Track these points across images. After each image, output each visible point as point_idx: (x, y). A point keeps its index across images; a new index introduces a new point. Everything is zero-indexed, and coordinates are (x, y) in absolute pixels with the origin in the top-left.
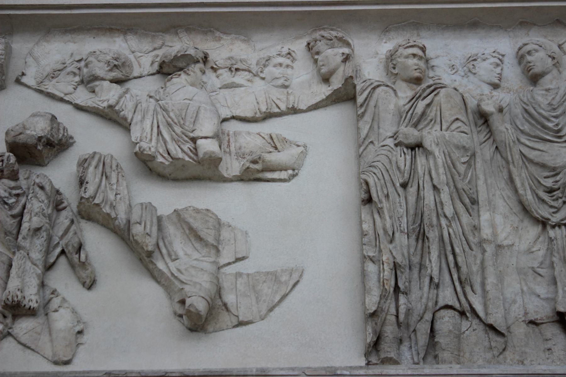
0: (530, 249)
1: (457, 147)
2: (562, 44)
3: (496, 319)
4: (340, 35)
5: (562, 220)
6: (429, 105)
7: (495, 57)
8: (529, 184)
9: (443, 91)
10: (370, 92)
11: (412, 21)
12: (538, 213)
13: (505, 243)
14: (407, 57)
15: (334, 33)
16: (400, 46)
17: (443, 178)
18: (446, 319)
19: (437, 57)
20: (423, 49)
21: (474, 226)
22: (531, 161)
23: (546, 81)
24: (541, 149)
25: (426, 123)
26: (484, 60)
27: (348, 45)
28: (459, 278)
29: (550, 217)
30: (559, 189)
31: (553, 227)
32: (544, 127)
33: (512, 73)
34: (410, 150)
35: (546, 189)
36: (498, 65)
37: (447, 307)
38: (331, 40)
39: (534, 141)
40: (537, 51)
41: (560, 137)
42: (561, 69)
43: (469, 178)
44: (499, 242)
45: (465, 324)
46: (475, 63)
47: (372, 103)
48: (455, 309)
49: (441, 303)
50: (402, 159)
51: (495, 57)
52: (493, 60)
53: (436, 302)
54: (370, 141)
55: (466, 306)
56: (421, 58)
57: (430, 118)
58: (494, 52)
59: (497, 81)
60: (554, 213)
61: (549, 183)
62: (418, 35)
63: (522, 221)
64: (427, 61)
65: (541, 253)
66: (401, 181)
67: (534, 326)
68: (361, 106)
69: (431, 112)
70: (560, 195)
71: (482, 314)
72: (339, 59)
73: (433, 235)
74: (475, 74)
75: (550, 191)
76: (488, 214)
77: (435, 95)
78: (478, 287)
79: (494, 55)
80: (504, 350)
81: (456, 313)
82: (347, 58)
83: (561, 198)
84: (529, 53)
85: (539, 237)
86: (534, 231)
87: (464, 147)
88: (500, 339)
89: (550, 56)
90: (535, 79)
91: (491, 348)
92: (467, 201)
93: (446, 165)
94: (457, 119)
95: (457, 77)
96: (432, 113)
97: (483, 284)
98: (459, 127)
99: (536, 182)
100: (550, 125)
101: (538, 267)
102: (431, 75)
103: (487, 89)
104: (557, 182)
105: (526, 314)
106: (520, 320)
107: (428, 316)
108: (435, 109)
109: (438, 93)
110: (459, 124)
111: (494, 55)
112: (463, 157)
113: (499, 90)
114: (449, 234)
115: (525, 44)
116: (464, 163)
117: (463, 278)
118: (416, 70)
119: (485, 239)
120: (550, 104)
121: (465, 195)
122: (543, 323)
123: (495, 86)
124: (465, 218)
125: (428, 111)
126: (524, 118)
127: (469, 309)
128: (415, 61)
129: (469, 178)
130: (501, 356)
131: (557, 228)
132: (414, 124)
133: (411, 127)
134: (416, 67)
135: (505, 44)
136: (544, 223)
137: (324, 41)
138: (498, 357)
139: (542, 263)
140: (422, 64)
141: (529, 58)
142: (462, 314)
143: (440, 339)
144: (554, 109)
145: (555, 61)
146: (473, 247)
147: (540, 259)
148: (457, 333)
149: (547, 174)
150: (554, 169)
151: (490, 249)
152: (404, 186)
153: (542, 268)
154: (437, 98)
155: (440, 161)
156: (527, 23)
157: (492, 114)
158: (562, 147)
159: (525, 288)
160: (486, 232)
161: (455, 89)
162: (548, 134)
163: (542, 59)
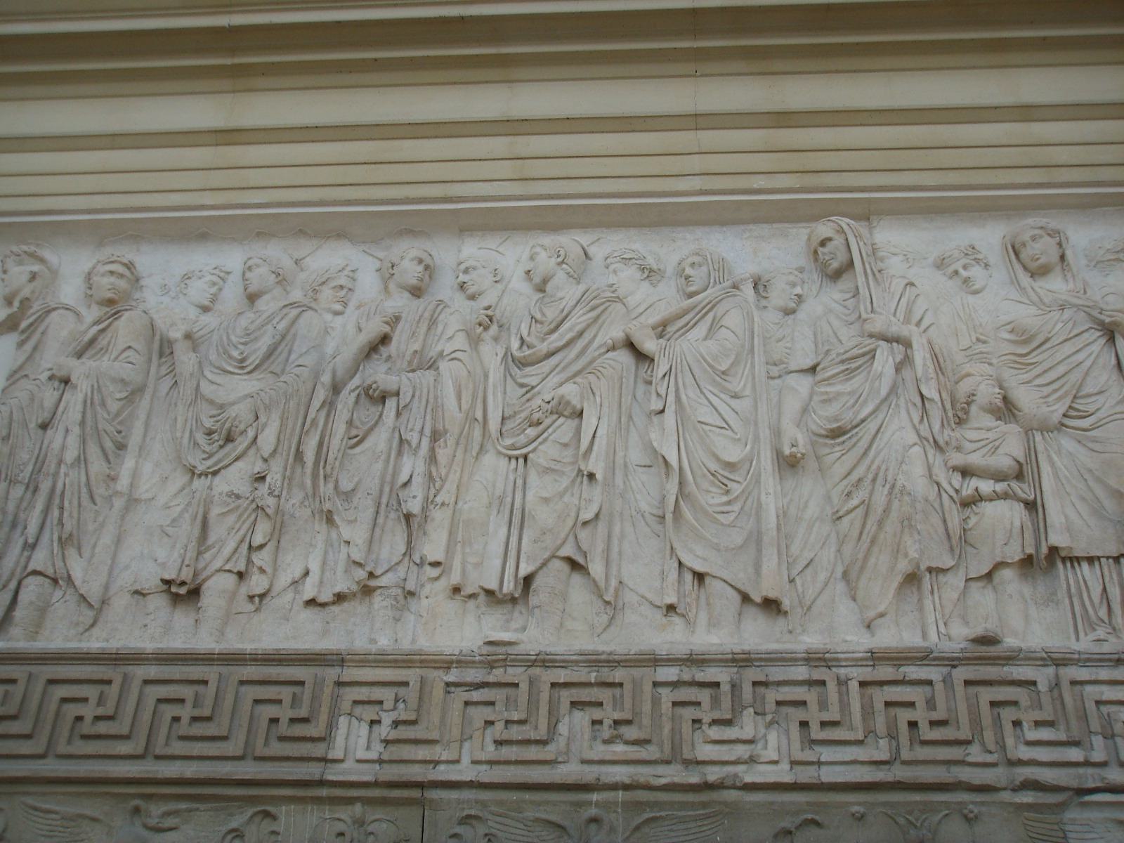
0: (166, 503)
1: (114, 380)
2: (301, 260)
3: (93, 590)
4: (33, 248)
5: (208, 468)
6: (103, 330)
7: (213, 274)
8: (192, 425)
9: (127, 314)
10: (40, 316)
11: (130, 233)
12: (187, 460)
13: (144, 496)
14: (103, 275)
15: (25, 248)
16: (99, 262)
17: (78, 417)
18: (32, 587)
19: (150, 275)
20: (130, 266)
21: (108, 476)
22: (203, 397)
23: (261, 304)
24: (218, 382)
25: (93, 352)
26: (200, 278)
27: (42, 261)
28: (60, 539)
29: (197, 464)
30: (216, 432)
31: (200, 476)
32: (230, 357)
33: (232, 295)
34: (63, 385)
35: (207, 432)
36: (214, 284)
37: (35, 573)
38: (19, 255)
39: (215, 373)
40: (258, 266)
41: (242, 368)
42: (288, 288)
43: (121, 418)
44: (137, 496)
45: (58, 594)
46: (187, 281)
47: (41, 329)
48: (46, 576)
49: (30, 568)
50: (49, 396)
51: (213, 274)
52: (209, 278)
53: (26, 567)
54: (23, 374)
55: (61, 572)
56: (122, 276)
57: (100, 346)
58: (215, 268)
59: (206, 303)
60: (203, 459)
61: (208, 423)
62: (138, 250)
63: (175, 469)
64: (137, 280)
65: (179, 509)
66: (40, 421)
67: (141, 597)
68: (23, 332)
69: (104, 338)
70: (216, 438)
71: (77, 583)
72: (25, 277)
73: (45, 486)
74: (185, 294)
75: (210, 433)
76: (133, 461)
77: (116, 319)
78: (87, 552)
79: (214, 272)
80: (92, 625)
81: (48, 580)
82: (33, 277)
83: (218, 441)
84: (250, 268)
85: (184, 489)
86: (180, 479)
87: (122, 380)
88: (91, 613)
89: (273, 272)
90: (252, 298)
91: (77, 624)
92: (109, 445)
93: (89, 402)
94: (130, 347)
95: (166, 299)
96: (103, 342)
97: (94, 546)
98: (129, 357)
99: (199, 423)
100: (235, 354)
101: (168, 526)
102: (135, 297)
103: (193, 313)
104: (217, 421)
105: (135, 582)
106: (126, 590)
107: (13, 585)
108: (110, 335)
109: (120, 316)
110: (129, 353)
111: (214, 272)
112: (120, 392)
113: (210, 314)
114: (65, 485)
115: (250, 259)
116: (120, 400)
117: (64, 536)
118: (109, 290)
119: (117, 492)
120: (246, 329)
121: (108, 438)
122: (150, 594)
123: (206, 309)
124: (97, 466)
125: (101, 338)
126: (217, 346)
127: (66, 575)
128: (112, 279)
129: (121, 418)
130: (87, 634)
131: (203, 477)
132: (76, 353)
133: (73, 356)
134: (110, 287)
135: (232, 258)
136: (192, 472)
137: (13, 257)
138: (82, 634)
139: (174, 520)
140: (122, 284)
141: (248, 275)
142: (55, 581)
143: (18, 614)
144: (248, 335)
145: (280, 278)
146: (98, 500)
147: (176, 515)
148: (41, 604)
149: (215, 412)
150: (222, 407)
151: (119, 503)
152: (44, 426)
153: (173, 527)
154: (116, 323)
155: (80, 397)
156: (265, 234)
157: (176, 341)
158: (241, 380)
159: (146, 551)
160: (123, 483)
161: (145, 312)
162: (230, 365)
163: (261, 275)
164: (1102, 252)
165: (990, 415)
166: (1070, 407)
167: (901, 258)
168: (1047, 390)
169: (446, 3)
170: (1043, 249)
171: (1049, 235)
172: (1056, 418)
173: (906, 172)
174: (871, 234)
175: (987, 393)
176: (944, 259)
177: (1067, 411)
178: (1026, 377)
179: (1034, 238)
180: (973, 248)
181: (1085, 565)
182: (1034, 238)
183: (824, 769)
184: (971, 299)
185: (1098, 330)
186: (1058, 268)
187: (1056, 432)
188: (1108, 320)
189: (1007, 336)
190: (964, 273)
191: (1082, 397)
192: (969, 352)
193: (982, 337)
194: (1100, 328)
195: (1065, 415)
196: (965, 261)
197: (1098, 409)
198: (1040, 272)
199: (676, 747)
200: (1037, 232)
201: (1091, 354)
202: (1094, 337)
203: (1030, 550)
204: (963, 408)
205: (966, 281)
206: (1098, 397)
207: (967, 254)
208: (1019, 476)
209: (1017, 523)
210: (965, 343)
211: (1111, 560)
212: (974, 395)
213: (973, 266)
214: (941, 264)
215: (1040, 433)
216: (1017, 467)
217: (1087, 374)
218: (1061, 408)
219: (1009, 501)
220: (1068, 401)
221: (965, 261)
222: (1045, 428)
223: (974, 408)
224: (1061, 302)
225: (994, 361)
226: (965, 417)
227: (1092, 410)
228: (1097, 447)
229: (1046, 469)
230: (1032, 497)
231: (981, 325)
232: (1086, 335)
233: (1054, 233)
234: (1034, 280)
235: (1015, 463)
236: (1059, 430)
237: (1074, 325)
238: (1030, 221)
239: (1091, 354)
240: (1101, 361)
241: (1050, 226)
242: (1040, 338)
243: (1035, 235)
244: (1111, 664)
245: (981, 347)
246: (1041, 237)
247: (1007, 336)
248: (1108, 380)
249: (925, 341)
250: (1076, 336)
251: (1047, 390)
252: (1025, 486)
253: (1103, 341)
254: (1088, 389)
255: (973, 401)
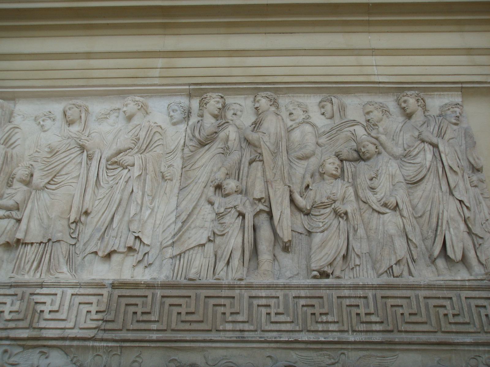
164: (100, 114)
165: (20, 183)
166: (52, 180)
167: (22, 116)
168: (45, 173)
169: (57, 2)
170: (73, 113)
171: (77, 107)
172: (42, 185)
173: (32, 80)
174: (15, 106)
175: (21, 172)
176: (36, 117)
177: (50, 181)
178: (43, 167)
179: (69, 109)
180: (51, 113)
181: (30, 246)
182: (69, 109)
183: (43, 331)
184: (43, 134)
185: (78, 147)
186: (78, 121)
187: (42, 190)
188: (81, 143)
189: (46, 149)
190: (42, 123)
191: (59, 176)
192: (32, 156)
193: (38, 150)
194: (80, 147)
195: (49, 183)
196: (44, 118)
197: (62, 181)
198: (70, 123)
199: (31, 322)
200: (73, 106)
201: (70, 158)
202: (76, 150)
203: (7, 240)
204: (11, 180)
205: (42, 126)
206: (65, 176)
207: (45, 115)
208: (18, 209)
209: (8, 228)
210: (31, 152)
211: (38, 244)
212: (15, 175)
213: (47, 120)
214: (36, 119)
215: (35, 191)
216: (16, 205)
217: (65, 166)
218: (47, 180)
219: (10, 219)
220: (50, 178)
221: (44, 118)
222: (37, 189)
223: (15, 180)
224: (69, 136)
225: (39, 160)
226: (11, 184)
227: (59, 182)
228: (52, 197)
229: (29, 206)
230: (20, 218)
231: (40, 145)
232: (73, 150)
233: (79, 107)
234: (69, 127)
235: (16, 203)
236: (43, 190)
237: (69, 145)
238: (70, 102)
239: (70, 158)
240: (74, 161)
241: (77, 103)
242: (55, 151)
243: (70, 107)
244: (9, 287)
245: (36, 155)
246: (73, 108)
247: (46, 149)
248: (72, 169)
249: (4, 152)
250: (68, 150)
251: (45, 173)
252: (18, 213)
253: (79, 152)
254: (63, 173)
255: (15, 177)
